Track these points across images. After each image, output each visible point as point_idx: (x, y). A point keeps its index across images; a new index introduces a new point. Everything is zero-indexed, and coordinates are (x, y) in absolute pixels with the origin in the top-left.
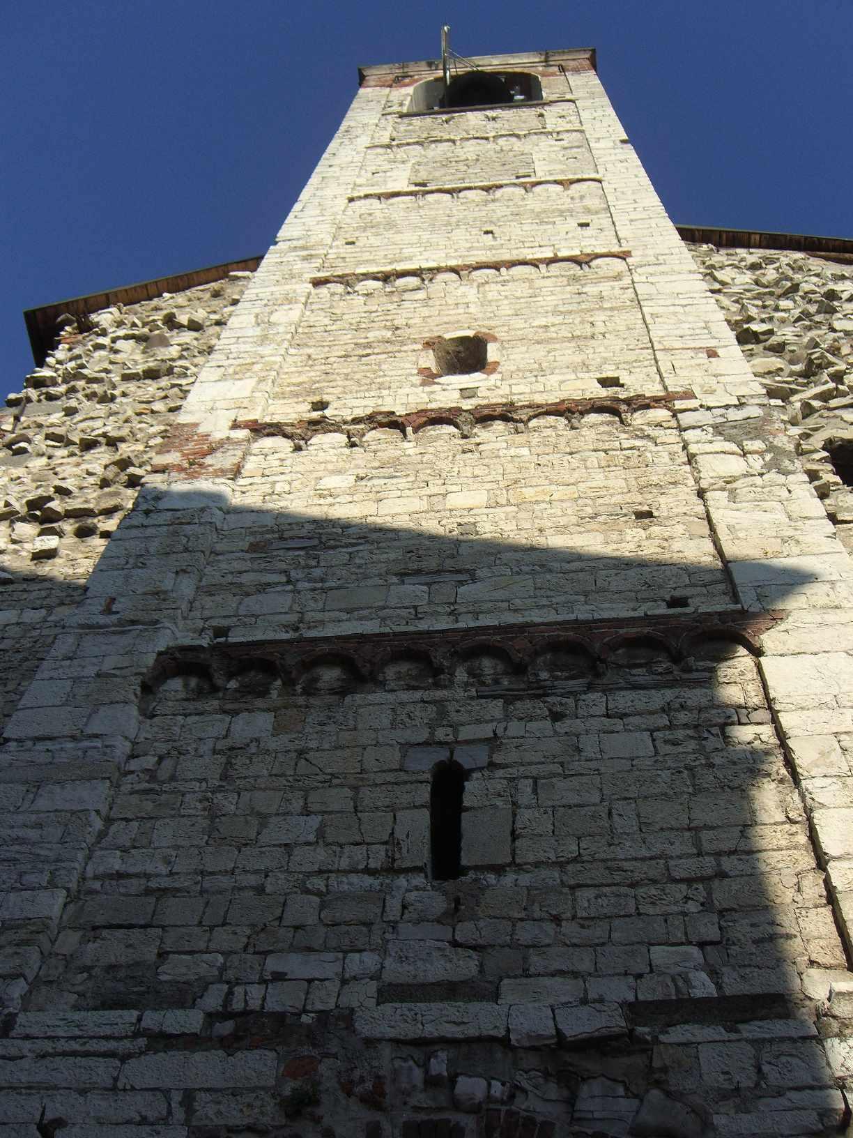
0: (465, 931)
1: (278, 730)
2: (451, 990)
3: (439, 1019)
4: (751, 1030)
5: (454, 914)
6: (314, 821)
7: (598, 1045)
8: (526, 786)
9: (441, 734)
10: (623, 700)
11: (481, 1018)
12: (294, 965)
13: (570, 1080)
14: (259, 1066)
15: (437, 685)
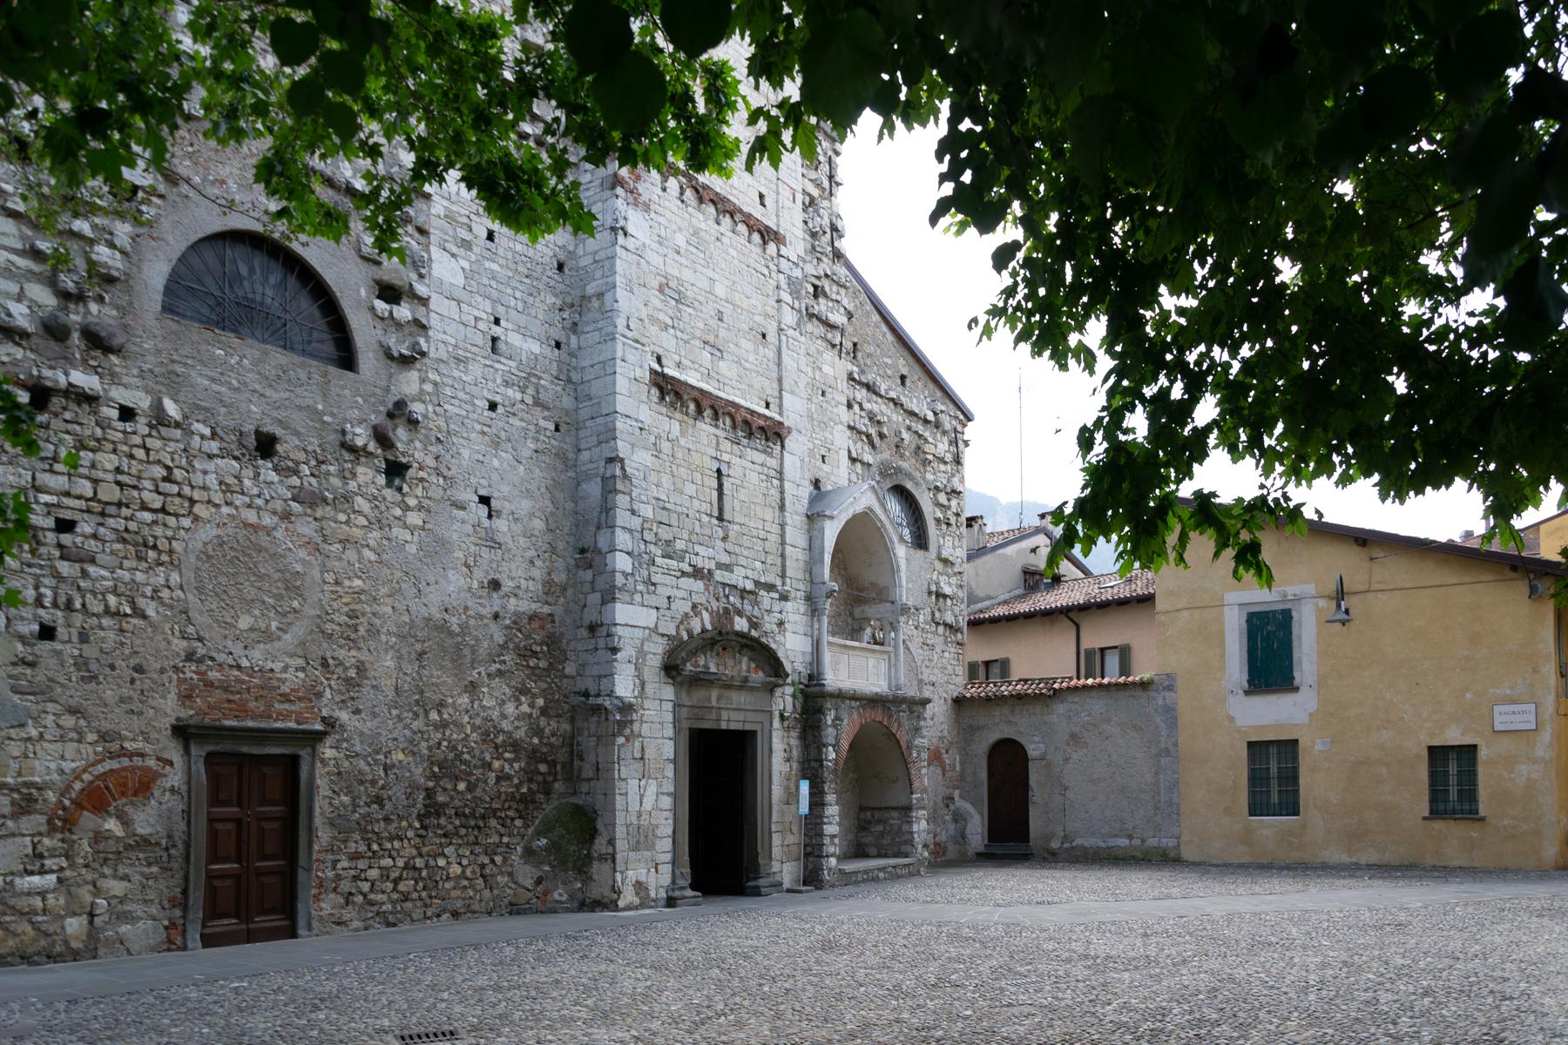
1: (683, 433)
5: (725, 539)
7: (750, 592)
13: (742, 598)
14: (699, 585)
15: (716, 426)
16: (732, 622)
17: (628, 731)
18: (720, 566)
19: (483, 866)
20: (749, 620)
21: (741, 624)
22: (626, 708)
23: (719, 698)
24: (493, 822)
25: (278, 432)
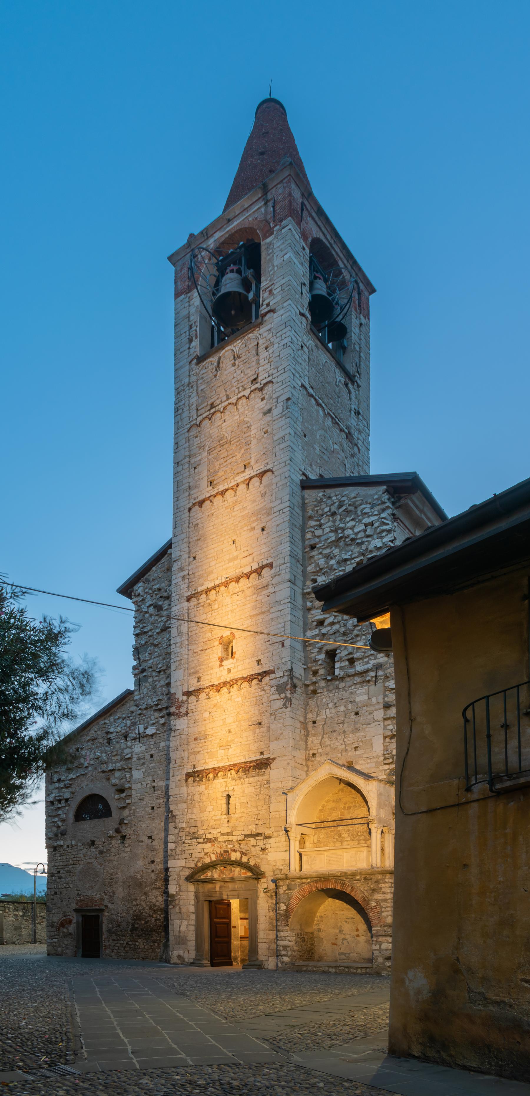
0: (230, 825)
2: (228, 834)
3: (226, 838)
4: (257, 838)
6: (212, 807)
8: (237, 799)
9: (227, 789)
10: (252, 780)
11: (230, 838)
12: (212, 831)
13: (240, 844)
14: (209, 845)
16: (229, 855)
17: (174, 904)
18: (223, 834)
19: (151, 946)
20: (241, 852)
21: (235, 856)
22: (173, 896)
23: (221, 887)
24: (154, 933)
25: (94, 839)
